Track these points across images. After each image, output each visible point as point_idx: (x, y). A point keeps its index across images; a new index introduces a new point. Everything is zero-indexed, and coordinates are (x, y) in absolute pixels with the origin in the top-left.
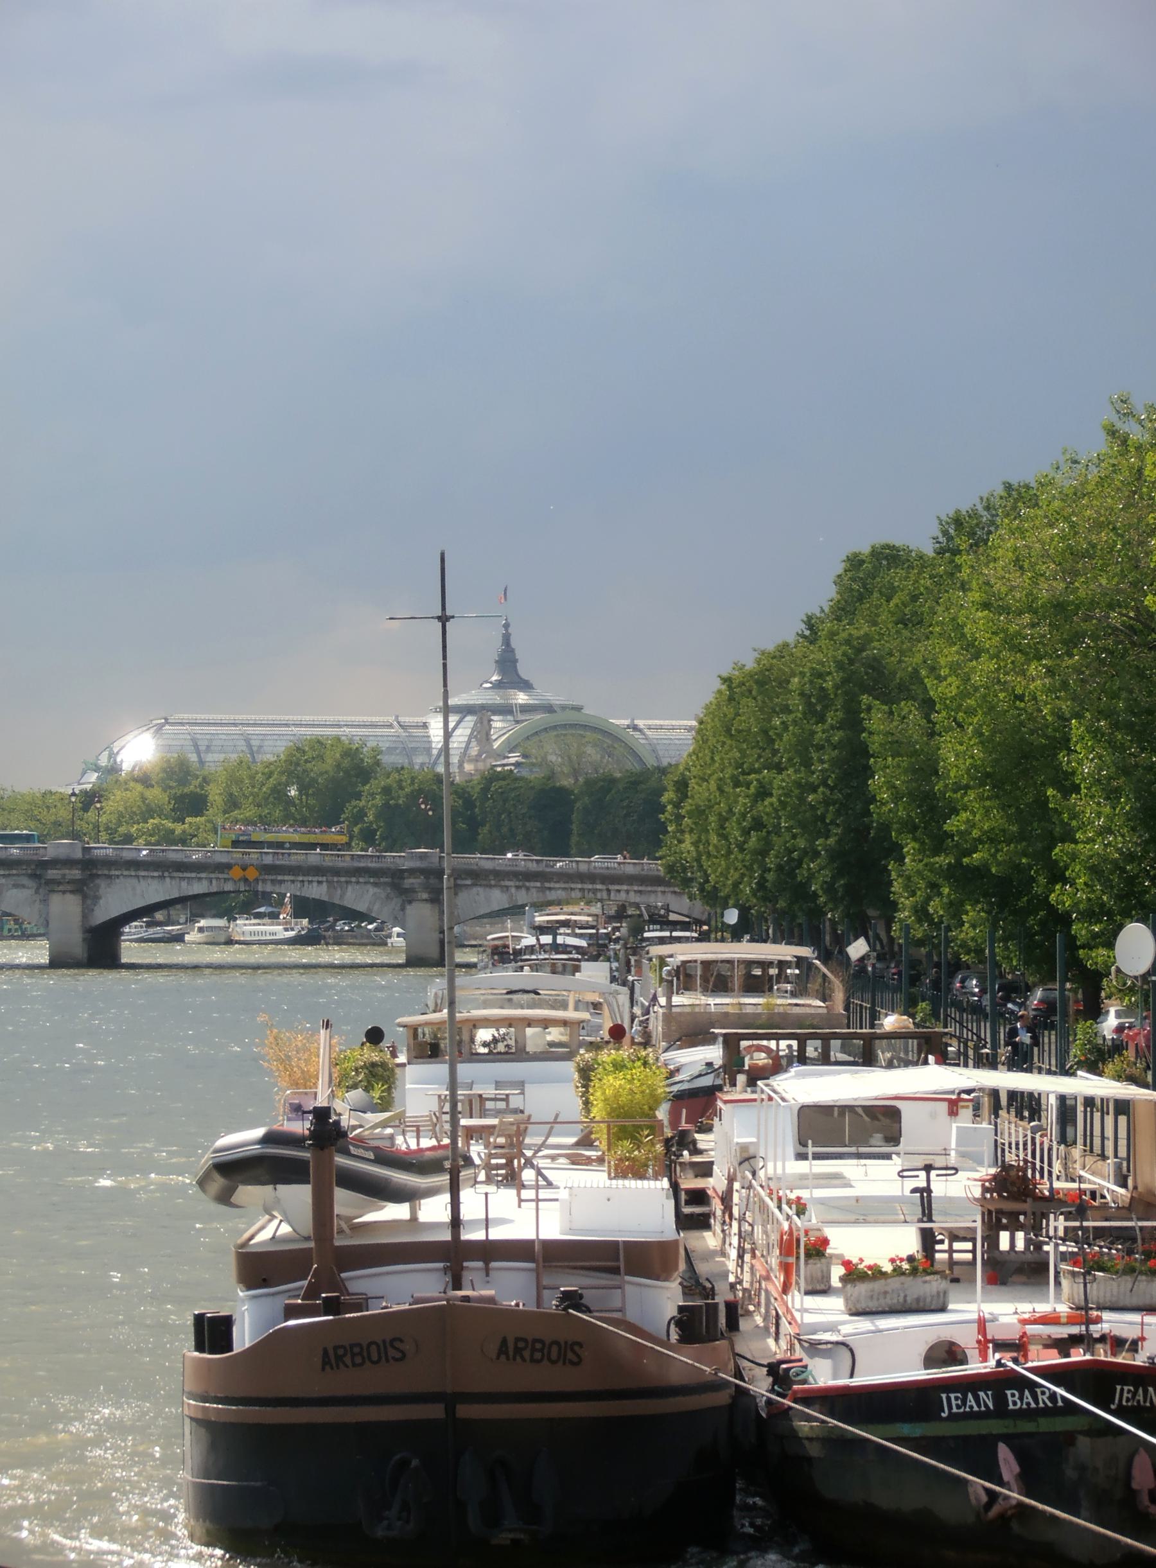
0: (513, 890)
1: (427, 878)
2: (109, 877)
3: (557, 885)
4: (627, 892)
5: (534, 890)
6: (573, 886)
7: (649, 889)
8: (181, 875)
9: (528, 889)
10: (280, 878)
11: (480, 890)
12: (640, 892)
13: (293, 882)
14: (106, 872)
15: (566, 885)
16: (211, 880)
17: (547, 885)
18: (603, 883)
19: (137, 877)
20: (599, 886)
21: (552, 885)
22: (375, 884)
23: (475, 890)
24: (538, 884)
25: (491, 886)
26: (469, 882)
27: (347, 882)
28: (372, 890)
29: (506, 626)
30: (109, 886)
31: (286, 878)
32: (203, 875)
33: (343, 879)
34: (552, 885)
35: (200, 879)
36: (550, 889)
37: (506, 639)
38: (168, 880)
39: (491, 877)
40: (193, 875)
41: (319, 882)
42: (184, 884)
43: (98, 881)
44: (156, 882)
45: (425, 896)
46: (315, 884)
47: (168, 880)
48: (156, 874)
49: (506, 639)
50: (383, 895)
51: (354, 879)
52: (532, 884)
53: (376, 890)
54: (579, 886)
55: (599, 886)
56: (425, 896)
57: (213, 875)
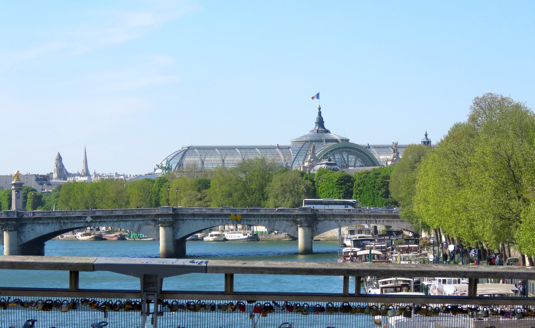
0: (339, 221)
1: (307, 218)
2: (183, 220)
3: (357, 219)
4: (383, 221)
5: (347, 221)
6: (362, 219)
7: (391, 220)
8: (211, 218)
9: (345, 221)
10: (250, 219)
11: (327, 222)
12: (388, 221)
13: (255, 220)
14: (182, 218)
15: (360, 219)
16: (223, 220)
17: (353, 219)
18: (374, 218)
19: (194, 220)
20: (372, 219)
21: (354, 219)
22: (287, 221)
23: (325, 222)
24: (349, 219)
25: (331, 220)
26: (323, 219)
27: (276, 220)
28: (285, 223)
29: (320, 109)
30: (183, 223)
31: (252, 219)
32: (220, 218)
33: (274, 219)
34: (354, 219)
35: (219, 220)
36: (354, 221)
37: (320, 113)
38: (206, 221)
39: (331, 216)
40: (216, 218)
41: (265, 220)
42: (212, 222)
43: (178, 222)
44: (201, 221)
45: (306, 225)
46: (263, 221)
47: (206, 221)
48: (201, 218)
49: (320, 113)
50: (290, 225)
51: (278, 219)
52: (347, 219)
53: (287, 223)
54: (365, 219)
55: (372, 219)
56: (306, 225)
57: (223, 219)
